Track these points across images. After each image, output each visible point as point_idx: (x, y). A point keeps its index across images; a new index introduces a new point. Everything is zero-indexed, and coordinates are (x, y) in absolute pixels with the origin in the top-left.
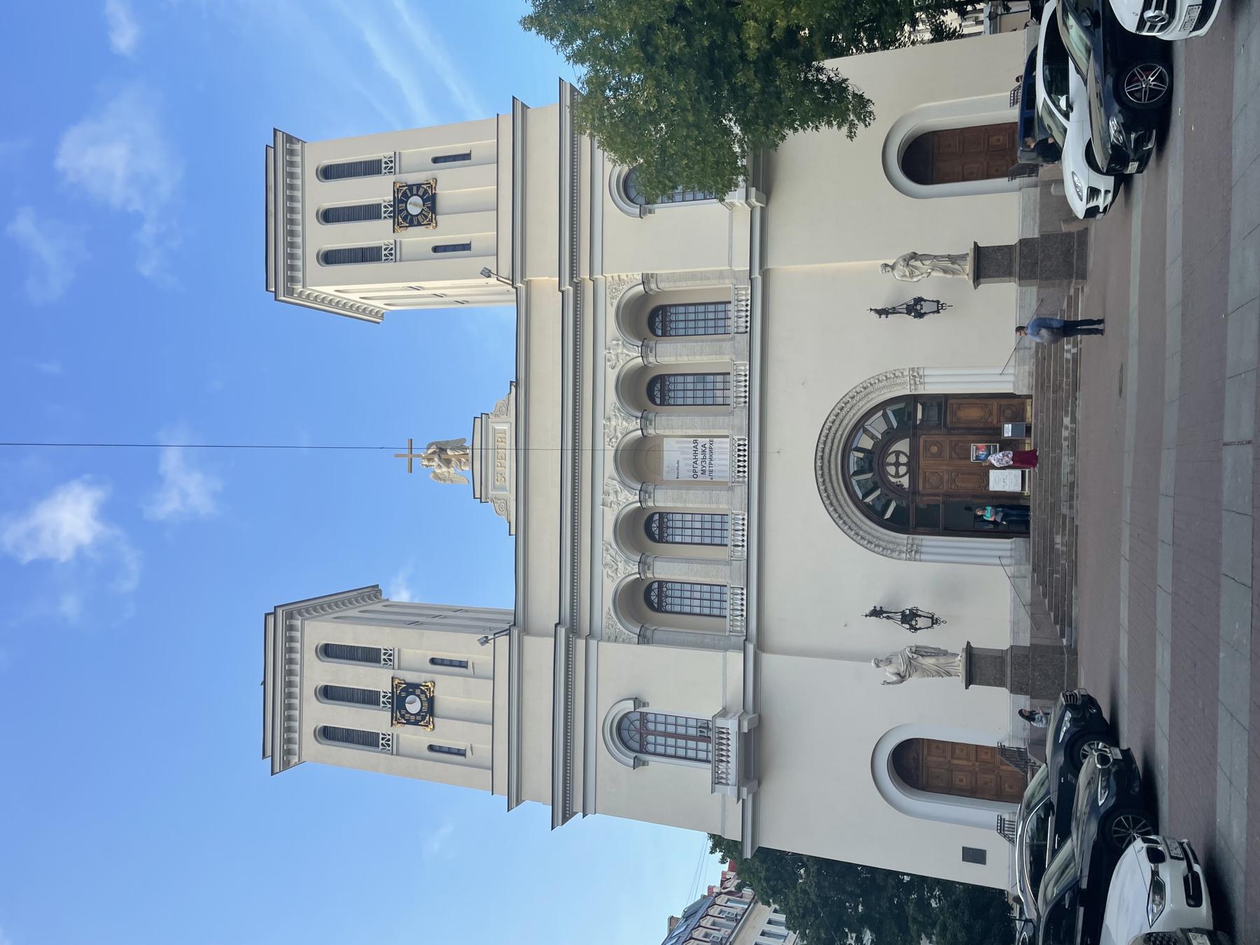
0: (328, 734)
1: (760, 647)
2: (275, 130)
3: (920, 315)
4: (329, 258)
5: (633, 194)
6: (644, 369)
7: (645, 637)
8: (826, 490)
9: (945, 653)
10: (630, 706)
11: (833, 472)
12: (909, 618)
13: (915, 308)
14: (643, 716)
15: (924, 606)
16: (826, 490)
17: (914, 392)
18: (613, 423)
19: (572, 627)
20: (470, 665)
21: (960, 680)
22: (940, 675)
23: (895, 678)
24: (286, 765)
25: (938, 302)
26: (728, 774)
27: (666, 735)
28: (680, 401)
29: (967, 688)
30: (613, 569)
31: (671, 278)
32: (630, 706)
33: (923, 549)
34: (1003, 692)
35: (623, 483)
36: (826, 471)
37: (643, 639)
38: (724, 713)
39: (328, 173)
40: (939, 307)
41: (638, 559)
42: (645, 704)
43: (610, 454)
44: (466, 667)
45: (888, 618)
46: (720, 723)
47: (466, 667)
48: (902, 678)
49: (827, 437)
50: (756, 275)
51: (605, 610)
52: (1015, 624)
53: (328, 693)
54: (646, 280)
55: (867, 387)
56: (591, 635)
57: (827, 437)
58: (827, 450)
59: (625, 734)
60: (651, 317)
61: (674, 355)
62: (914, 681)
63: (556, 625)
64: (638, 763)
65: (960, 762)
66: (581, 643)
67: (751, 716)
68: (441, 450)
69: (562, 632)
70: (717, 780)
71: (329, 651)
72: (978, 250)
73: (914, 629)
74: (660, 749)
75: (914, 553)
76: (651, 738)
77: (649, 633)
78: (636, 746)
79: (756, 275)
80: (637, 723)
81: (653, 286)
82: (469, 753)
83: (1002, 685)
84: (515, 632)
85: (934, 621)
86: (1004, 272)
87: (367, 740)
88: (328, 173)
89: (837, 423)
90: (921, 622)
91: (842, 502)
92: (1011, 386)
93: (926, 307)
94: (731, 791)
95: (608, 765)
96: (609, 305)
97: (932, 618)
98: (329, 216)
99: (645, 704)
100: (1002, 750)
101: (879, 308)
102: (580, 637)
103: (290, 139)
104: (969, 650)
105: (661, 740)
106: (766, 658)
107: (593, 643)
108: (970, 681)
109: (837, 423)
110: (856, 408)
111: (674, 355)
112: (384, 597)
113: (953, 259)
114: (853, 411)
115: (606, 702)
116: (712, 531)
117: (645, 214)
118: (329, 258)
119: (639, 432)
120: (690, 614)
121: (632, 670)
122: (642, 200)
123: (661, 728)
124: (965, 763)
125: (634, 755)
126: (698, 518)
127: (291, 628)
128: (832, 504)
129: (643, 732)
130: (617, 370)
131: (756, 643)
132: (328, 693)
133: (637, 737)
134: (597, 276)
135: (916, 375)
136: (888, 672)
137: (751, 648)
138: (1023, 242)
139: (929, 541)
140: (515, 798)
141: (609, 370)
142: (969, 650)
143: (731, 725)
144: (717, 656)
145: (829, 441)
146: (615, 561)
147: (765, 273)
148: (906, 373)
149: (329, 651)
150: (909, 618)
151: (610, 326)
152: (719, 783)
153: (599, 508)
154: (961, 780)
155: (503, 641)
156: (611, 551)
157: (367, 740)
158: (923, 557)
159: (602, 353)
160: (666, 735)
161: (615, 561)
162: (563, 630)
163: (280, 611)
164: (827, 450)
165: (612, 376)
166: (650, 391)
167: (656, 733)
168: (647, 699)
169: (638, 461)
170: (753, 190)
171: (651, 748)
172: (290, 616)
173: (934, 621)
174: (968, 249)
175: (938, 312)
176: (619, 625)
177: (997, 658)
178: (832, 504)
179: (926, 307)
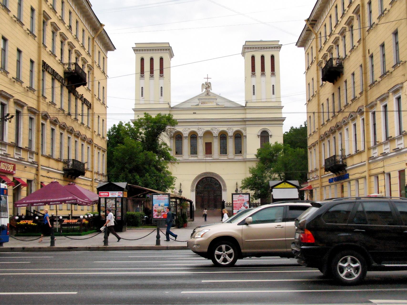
0: (142, 60)
4: (253, 58)
24: (134, 50)
53: (152, 59)
55: (223, 181)
60: (239, 136)
68: (209, 87)
71: (161, 59)
75: (192, 191)
88: (273, 57)
98: (263, 57)
103: (280, 48)
112: (172, 59)
118: (253, 58)
130: (227, 131)
135: (225, 190)
139: (194, 193)
147: (246, 161)
149: (161, 59)
151: (236, 128)
153: (197, 127)
166: (223, 136)
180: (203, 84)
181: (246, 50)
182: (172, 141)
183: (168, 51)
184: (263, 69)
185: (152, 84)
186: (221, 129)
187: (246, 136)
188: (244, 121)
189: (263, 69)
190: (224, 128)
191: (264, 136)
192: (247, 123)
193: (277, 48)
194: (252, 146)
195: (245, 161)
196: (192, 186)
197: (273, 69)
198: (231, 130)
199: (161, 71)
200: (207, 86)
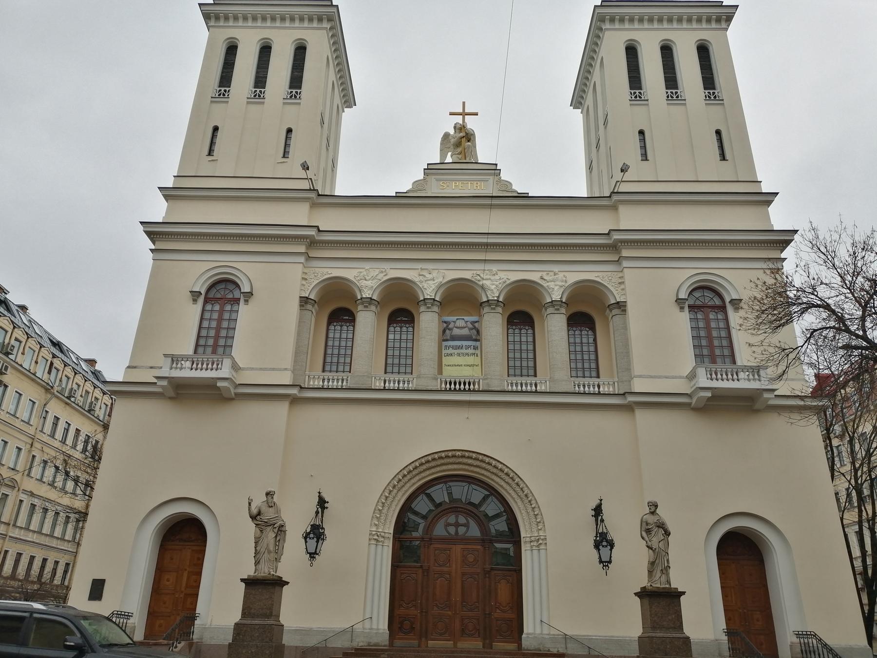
0: (232, 50)
1: (294, 401)
2: (737, 6)
3: (597, 546)
4: (632, 52)
5: (697, 294)
6: (541, 306)
7: (306, 303)
8: (434, 459)
9: (277, 560)
10: (246, 288)
11: (450, 467)
12: (316, 533)
13: (603, 541)
14: (237, 301)
15: (326, 547)
16: (434, 459)
17: (523, 540)
18: (493, 278)
19: (314, 243)
20: (284, 160)
21: (249, 571)
22: (256, 553)
23: (255, 511)
24: (207, 17)
25: (610, 562)
26: (181, 369)
27: (220, 319)
28: (511, 339)
29: (242, 580)
30: (368, 278)
31: (625, 327)
32: (246, 288)
33: (380, 547)
34: (236, 616)
35: (440, 286)
36: (451, 460)
37: (304, 301)
38: (235, 367)
39: (703, 51)
40: (606, 563)
41: (375, 297)
42: (246, 301)
43: (467, 275)
44: (284, 157)
45: (317, 513)
46: (227, 362)
47: (284, 157)
48: (253, 518)
49: (482, 461)
50: (631, 399)
51: (330, 271)
52: (308, 632)
53: (265, 51)
54: (621, 306)
55: (527, 497)
56: (309, 258)
57: (482, 461)
58: (470, 461)
59: (223, 286)
60: (587, 314)
61: (554, 329)
62: (251, 526)
63: (318, 227)
64: (195, 295)
65: (185, 579)
66: (302, 249)
67: (233, 391)
69: (312, 232)
70: (175, 359)
71: (300, 51)
72: (676, 595)
73: (306, 537)
74: (207, 315)
75: (376, 539)
76: (217, 307)
77: (309, 307)
78: (211, 295)
79: (631, 399)
80: (230, 296)
81: (615, 311)
82: (211, 158)
83: (244, 615)
84: (313, 195)
85: (313, 555)
86: (651, 622)
87: (226, 79)
89: (495, 470)
90: (312, 543)
91: (423, 475)
92: (531, 631)
93: (605, 551)
94: (166, 372)
95: (196, 272)
96: (597, 274)
97: (315, 553)
98: (667, 51)
99: (246, 301)
100: (191, 617)
101: (603, 507)
102: (307, 249)
103: (729, 19)
104: (280, 583)
105: (215, 316)
106: (283, 408)
107: (302, 259)
108: (250, 583)
109: (495, 470)
110: (508, 488)
111: (554, 329)
113: (666, 570)
114: (505, 485)
115: (249, 270)
116: (398, 361)
117: (679, 304)
118: (632, 52)
119: (485, 299)
120: (325, 354)
121: (277, 291)
122: (691, 302)
123: (226, 316)
124: (184, 585)
125: (203, 292)
126: (410, 345)
127: (320, 20)
128: (421, 464)
129: (223, 301)
131: (296, 397)
132: (265, 51)
133: (219, 296)
134: (625, 264)
135: (539, 543)
136: (259, 500)
137: (294, 391)
138: (687, 639)
139: (386, 553)
140: (169, 194)
141: (540, 274)
142: (280, 583)
143: (225, 371)
144: (288, 362)
145: (478, 463)
146: (373, 278)
147: (629, 408)
148: (541, 533)
149: (300, 51)
150: (316, 533)
152: (173, 360)
154: (168, 580)
155: (306, 185)
156: (382, 275)
157: (226, 79)
158: (373, 547)
159: (556, 268)
160: (220, 319)
161: (373, 278)
162: (313, 233)
163: (335, 10)
164: (470, 461)
165: (534, 277)
167: (221, 312)
168: (252, 301)
169: (461, 297)
170: (709, 394)
171: (209, 307)
172: (330, 20)
173: (313, 555)
174: (677, 583)
175: (601, 562)
176: (316, 282)
177: (272, 612)
178: (421, 464)
179: (605, 551)
180: (446, 136)
181: (607, 25)
182: (310, 317)
183: (326, 25)
184: (671, 80)
185: (256, 123)
186: (514, 277)
187: (621, 306)
188: (613, 247)
189: (671, 80)
190: (533, 275)
191: (707, 304)
192: (625, 253)
193: (718, 20)
194: (657, 346)
195: (629, 404)
196: (378, 513)
197: (709, 81)
198: (557, 280)
199: (296, 81)
200: (462, 140)
